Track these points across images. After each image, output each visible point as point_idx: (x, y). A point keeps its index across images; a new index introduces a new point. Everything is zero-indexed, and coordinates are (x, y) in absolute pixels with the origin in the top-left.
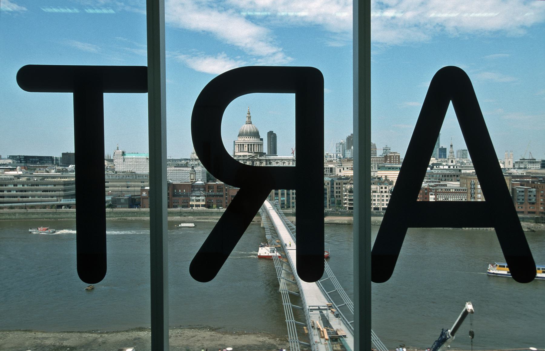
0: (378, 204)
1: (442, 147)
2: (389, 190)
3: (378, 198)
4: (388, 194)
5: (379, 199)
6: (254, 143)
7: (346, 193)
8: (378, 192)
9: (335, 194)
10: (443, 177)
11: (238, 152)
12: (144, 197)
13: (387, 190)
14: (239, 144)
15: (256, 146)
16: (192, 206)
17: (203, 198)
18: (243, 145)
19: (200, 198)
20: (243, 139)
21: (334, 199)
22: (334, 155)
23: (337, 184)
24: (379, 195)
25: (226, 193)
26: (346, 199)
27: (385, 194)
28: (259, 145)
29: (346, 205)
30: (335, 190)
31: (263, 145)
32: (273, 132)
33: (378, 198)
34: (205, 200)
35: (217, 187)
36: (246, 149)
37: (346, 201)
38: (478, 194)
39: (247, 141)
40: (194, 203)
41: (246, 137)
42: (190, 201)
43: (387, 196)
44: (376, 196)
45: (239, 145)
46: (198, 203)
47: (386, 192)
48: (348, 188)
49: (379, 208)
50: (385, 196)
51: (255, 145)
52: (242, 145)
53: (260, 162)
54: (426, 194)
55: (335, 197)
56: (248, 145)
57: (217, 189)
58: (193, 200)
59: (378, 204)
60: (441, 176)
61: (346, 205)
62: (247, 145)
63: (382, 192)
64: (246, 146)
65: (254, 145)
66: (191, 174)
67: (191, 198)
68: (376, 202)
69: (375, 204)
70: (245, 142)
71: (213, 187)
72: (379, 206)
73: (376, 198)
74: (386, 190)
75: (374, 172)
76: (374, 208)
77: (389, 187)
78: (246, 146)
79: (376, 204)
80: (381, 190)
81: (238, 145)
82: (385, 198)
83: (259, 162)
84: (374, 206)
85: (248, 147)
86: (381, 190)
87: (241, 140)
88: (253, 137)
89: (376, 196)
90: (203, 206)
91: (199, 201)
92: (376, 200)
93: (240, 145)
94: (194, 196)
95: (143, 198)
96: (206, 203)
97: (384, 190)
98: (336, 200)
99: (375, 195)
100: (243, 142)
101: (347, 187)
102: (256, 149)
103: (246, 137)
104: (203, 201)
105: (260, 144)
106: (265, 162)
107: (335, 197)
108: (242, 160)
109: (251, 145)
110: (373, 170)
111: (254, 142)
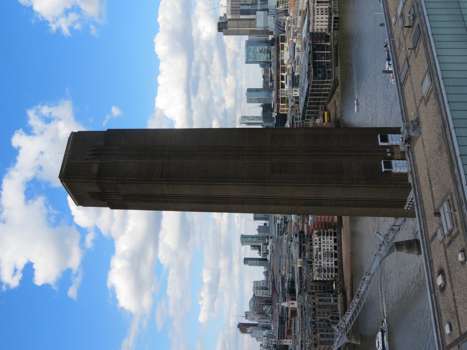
1: (257, 230)
2: (318, 237)
3: (326, 246)
4: (322, 238)
5: (327, 246)
7: (323, 276)
13: (318, 238)
22: (264, 340)
23: (312, 289)
24: (323, 246)
27: (322, 240)
29: (334, 276)
43: (324, 239)
44: (324, 248)
47: (320, 240)
48: (317, 273)
49: (334, 246)
50: (324, 240)
55: (325, 291)
61: (334, 276)
63: (320, 244)
68: (330, 248)
69: (331, 250)
72: (333, 246)
73: (326, 248)
74: (318, 240)
75: (297, 262)
76: (334, 250)
79: (331, 248)
80: (318, 244)
82: (325, 240)
84: (333, 250)
86: (318, 244)
89: (324, 248)
97: (318, 242)
98: (328, 289)
101: (316, 274)
107: (325, 291)
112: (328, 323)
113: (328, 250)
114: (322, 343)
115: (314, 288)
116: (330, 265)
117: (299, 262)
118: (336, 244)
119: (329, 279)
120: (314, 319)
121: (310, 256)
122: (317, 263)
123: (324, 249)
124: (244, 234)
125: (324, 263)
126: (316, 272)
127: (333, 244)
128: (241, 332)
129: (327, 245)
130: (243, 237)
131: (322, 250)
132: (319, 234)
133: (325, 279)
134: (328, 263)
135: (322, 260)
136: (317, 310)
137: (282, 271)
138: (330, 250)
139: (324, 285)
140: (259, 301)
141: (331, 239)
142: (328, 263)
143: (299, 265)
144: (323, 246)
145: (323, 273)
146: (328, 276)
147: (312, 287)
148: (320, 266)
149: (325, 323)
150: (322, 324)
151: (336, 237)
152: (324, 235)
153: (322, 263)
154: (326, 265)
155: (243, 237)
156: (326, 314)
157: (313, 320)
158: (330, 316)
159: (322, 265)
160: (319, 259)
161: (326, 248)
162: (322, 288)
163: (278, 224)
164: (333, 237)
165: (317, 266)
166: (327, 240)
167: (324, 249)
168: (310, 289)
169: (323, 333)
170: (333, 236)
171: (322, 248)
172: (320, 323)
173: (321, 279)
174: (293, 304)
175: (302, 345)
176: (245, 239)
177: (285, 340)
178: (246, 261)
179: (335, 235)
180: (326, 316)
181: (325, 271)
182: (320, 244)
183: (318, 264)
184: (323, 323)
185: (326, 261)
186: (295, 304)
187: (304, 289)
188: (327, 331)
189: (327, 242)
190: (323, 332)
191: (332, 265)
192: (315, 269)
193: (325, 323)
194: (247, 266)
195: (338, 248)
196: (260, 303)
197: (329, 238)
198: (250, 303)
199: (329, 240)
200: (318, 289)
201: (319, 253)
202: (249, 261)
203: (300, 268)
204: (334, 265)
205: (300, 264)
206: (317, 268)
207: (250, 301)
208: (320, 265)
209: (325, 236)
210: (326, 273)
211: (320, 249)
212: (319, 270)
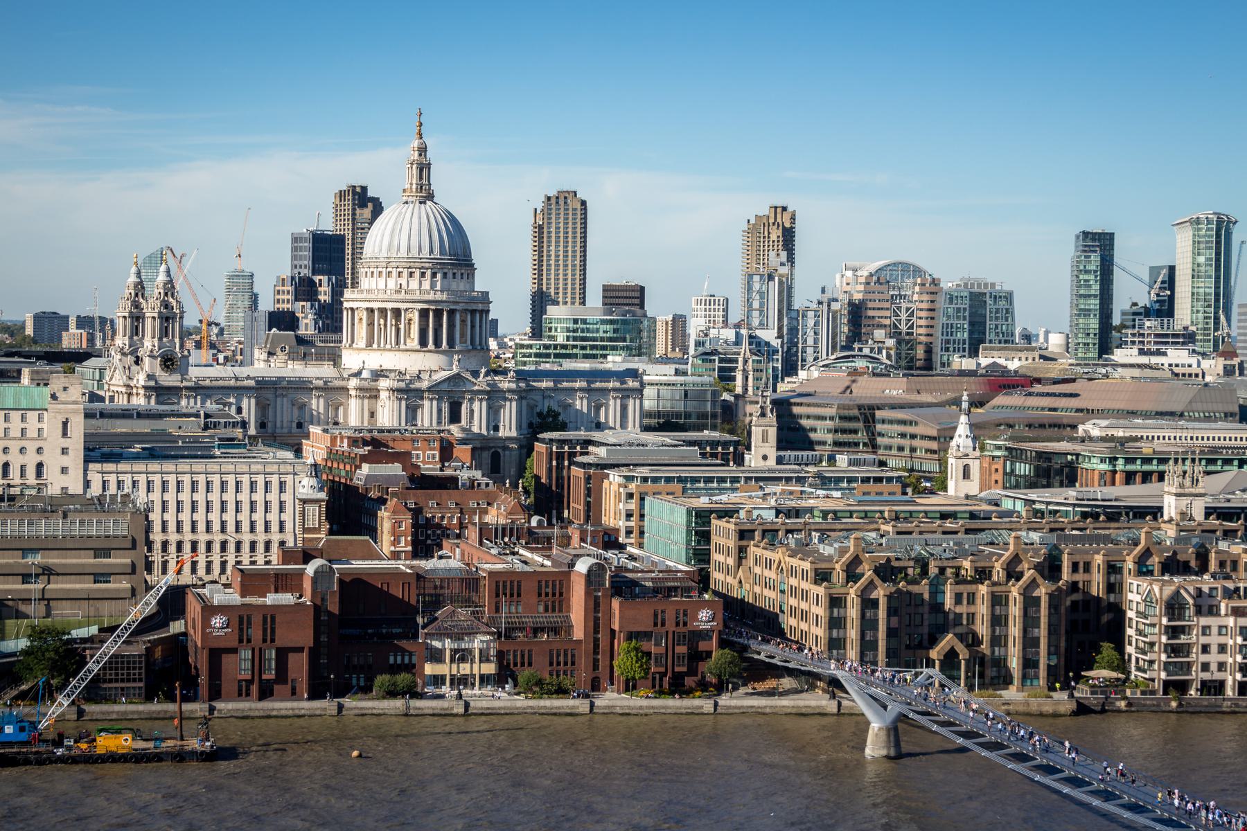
15: (463, 321)
16: (438, 680)
28: (478, 315)
31: (488, 311)
32: (364, 189)
35: (540, 587)
39: (417, 297)
41: (411, 275)
45: (370, 311)
46: (465, 668)
51: (458, 316)
53: (489, 408)
56: (424, 314)
58: (436, 656)
62: (416, 317)
65: (451, 313)
66: (305, 502)
70: (409, 297)
81: (364, 315)
83: (484, 404)
85: (420, 325)
90: (485, 680)
91: (462, 656)
93: (376, 312)
100: (395, 297)
102: (463, 335)
105: (480, 307)
106: (514, 404)
109: (438, 314)
110: (1187, 491)
112: (925, 637)
114: (836, 602)
116: (1204, 658)
119: (1130, 649)
120: (942, 570)
121: (1235, 564)
125: (1215, 630)
126: (1169, 590)
128: (753, 221)
133: (1130, 632)
135: (1231, 621)
136: (983, 589)
137: (1104, 423)
140: (914, 306)
142: (1214, 649)
143: (1171, 506)
147: (1087, 567)
149: (926, 623)
150: (920, 610)
154: (1203, 640)
157: (936, 571)
159: (1204, 621)
168: (1077, 558)
169: (882, 613)
174: (966, 474)
175: (797, 513)
177: (773, 432)
184: (926, 616)
185: (1222, 640)
186: (966, 483)
187: (1063, 530)
188: (891, 633)
190: (889, 615)
191: (1205, 667)
192: (1187, 585)
194: (1068, 250)
202: (1095, 258)
203: (1156, 512)
204: (1206, 676)
205: (1183, 514)
208: (1205, 609)
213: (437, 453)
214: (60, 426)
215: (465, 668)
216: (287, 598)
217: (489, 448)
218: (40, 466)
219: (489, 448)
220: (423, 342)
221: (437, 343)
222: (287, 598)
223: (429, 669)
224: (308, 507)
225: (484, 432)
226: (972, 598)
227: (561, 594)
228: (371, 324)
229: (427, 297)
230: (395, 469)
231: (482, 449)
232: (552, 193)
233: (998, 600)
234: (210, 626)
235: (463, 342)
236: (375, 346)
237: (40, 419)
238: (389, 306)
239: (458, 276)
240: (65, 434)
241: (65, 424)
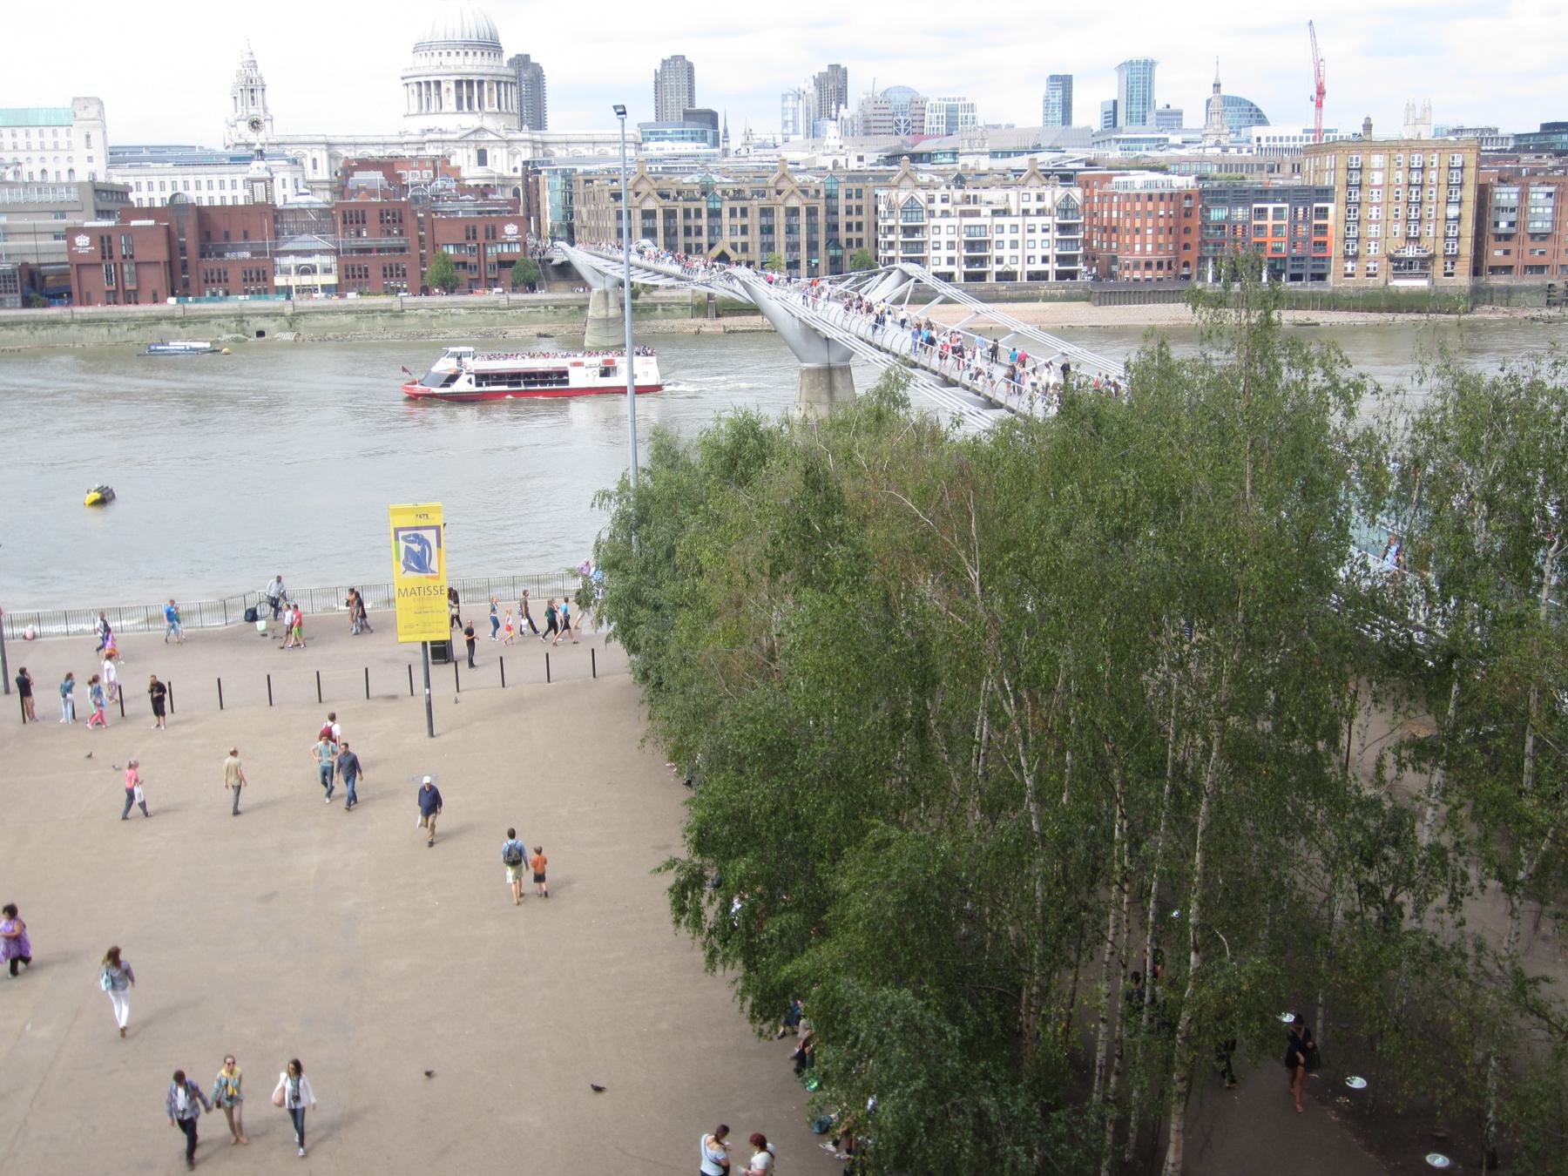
0: (1014, 260)
1: (1168, 106)
4: (1047, 220)
6: (481, 78)
7: (891, 222)
8: (1014, 213)
9: (843, 235)
10: (1220, 170)
11: (419, 114)
12: (82, 261)
13: (1047, 203)
14: (422, 79)
15: (490, 90)
16: (287, 291)
17: (329, 260)
18: (438, 83)
19: (316, 260)
20: (436, 60)
21: (839, 252)
25: (420, 237)
26: (891, 245)
27: (1040, 222)
30: (842, 219)
32: (527, 56)
33: (1015, 237)
34: (334, 267)
35: (382, 215)
36: (450, 100)
37: (891, 253)
38: (1372, 205)
39: (453, 70)
40: (294, 280)
41: (449, 54)
42: (274, 273)
45: (419, 84)
46: (307, 280)
47: (1040, 212)
50: (1039, 229)
51: (485, 85)
52: (432, 85)
53: (509, 153)
54: (1186, 215)
55: (844, 245)
56: (459, 83)
57: (382, 222)
58: (287, 271)
59: (1014, 260)
60: (1215, 168)
62: (453, 86)
63: (1026, 212)
64: (448, 89)
66: (253, 181)
67: (277, 260)
68: (1006, 253)
69: (999, 261)
70: (446, 71)
71: (364, 215)
72: (1014, 268)
74: (1040, 205)
77: (1053, 193)
78: (448, 89)
79: (1006, 261)
81: (415, 87)
82: (1039, 236)
84: (999, 268)
86: (1024, 206)
87: (429, 66)
88: (475, 54)
89: (1007, 229)
92: (1007, 244)
94: (287, 253)
95: (78, 265)
96: (340, 279)
97: (1034, 206)
98: (848, 258)
99: (1003, 227)
102: (490, 100)
103: (449, 54)
104: (327, 271)
105: (505, 79)
107: (844, 245)
108: (436, 144)
111: (480, 70)
112: (705, 246)
113: (1000, 244)
115: (854, 202)
117: (977, 163)
118: (1022, 279)
122: (944, 200)
123: (1001, 228)
124: (1159, 76)
125: (943, 229)
127: (1023, 268)
129: (1020, 244)
130: (1148, 66)
131: (999, 220)
132: (1065, 209)
134: (944, 245)
138: (997, 253)
139: (865, 242)
141: (1045, 260)
142: (944, 245)
144: (1017, 226)
145: (901, 222)
146: (891, 245)
148: (932, 214)
149: (705, 233)
150: (699, 222)
151: (1052, 278)
152: (1063, 228)
153: (943, 222)
154: (934, 238)
155: (1148, 66)
156: (740, 239)
157: (719, 193)
158: (729, 252)
159: (934, 222)
160: (961, 207)
161: (1007, 237)
162: (854, 235)
163: (1166, 140)
164: (1052, 267)
165: (931, 201)
166: (1038, 244)
167: (1001, 228)
170: (1056, 266)
171: (1006, 221)
172: (705, 215)
173: (880, 223)
176: (1139, 75)
178: (1063, 84)
179: (1061, 276)
180: (734, 239)
181: (908, 231)
182: (1026, 212)
183: (938, 206)
185: (952, 238)
189: (1031, 244)
193: (705, 233)
194: (1041, 89)
195: (1003, 286)
196: (902, 126)
197: (1047, 252)
198: (902, 90)
199: (1039, 253)
200: (849, 219)
201: (986, 211)
202: (1059, 93)
206: (921, 196)
207: (909, 90)
208: (938, 213)
209: (1057, 235)
210: (901, 238)
211: (1005, 213)
212: (911, 208)
213: (431, 172)
214: (84, 139)
215: (307, 280)
216: (151, 222)
217: (510, 186)
218: (71, 171)
219: (510, 186)
220: (459, 106)
221: (470, 106)
222: (151, 222)
223: (279, 281)
224: (255, 185)
225: (506, 174)
226: (744, 212)
227: (401, 221)
228: (420, 95)
229: (460, 71)
230: (377, 177)
231: (503, 186)
232: (667, 56)
233: (766, 212)
234: (75, 245)
235: (491, 105)
236: (424, 111)
237: (68, 134)
238: (431, 79)
239: (486, 54)
240: (88, 146)
241: (88, 137)
